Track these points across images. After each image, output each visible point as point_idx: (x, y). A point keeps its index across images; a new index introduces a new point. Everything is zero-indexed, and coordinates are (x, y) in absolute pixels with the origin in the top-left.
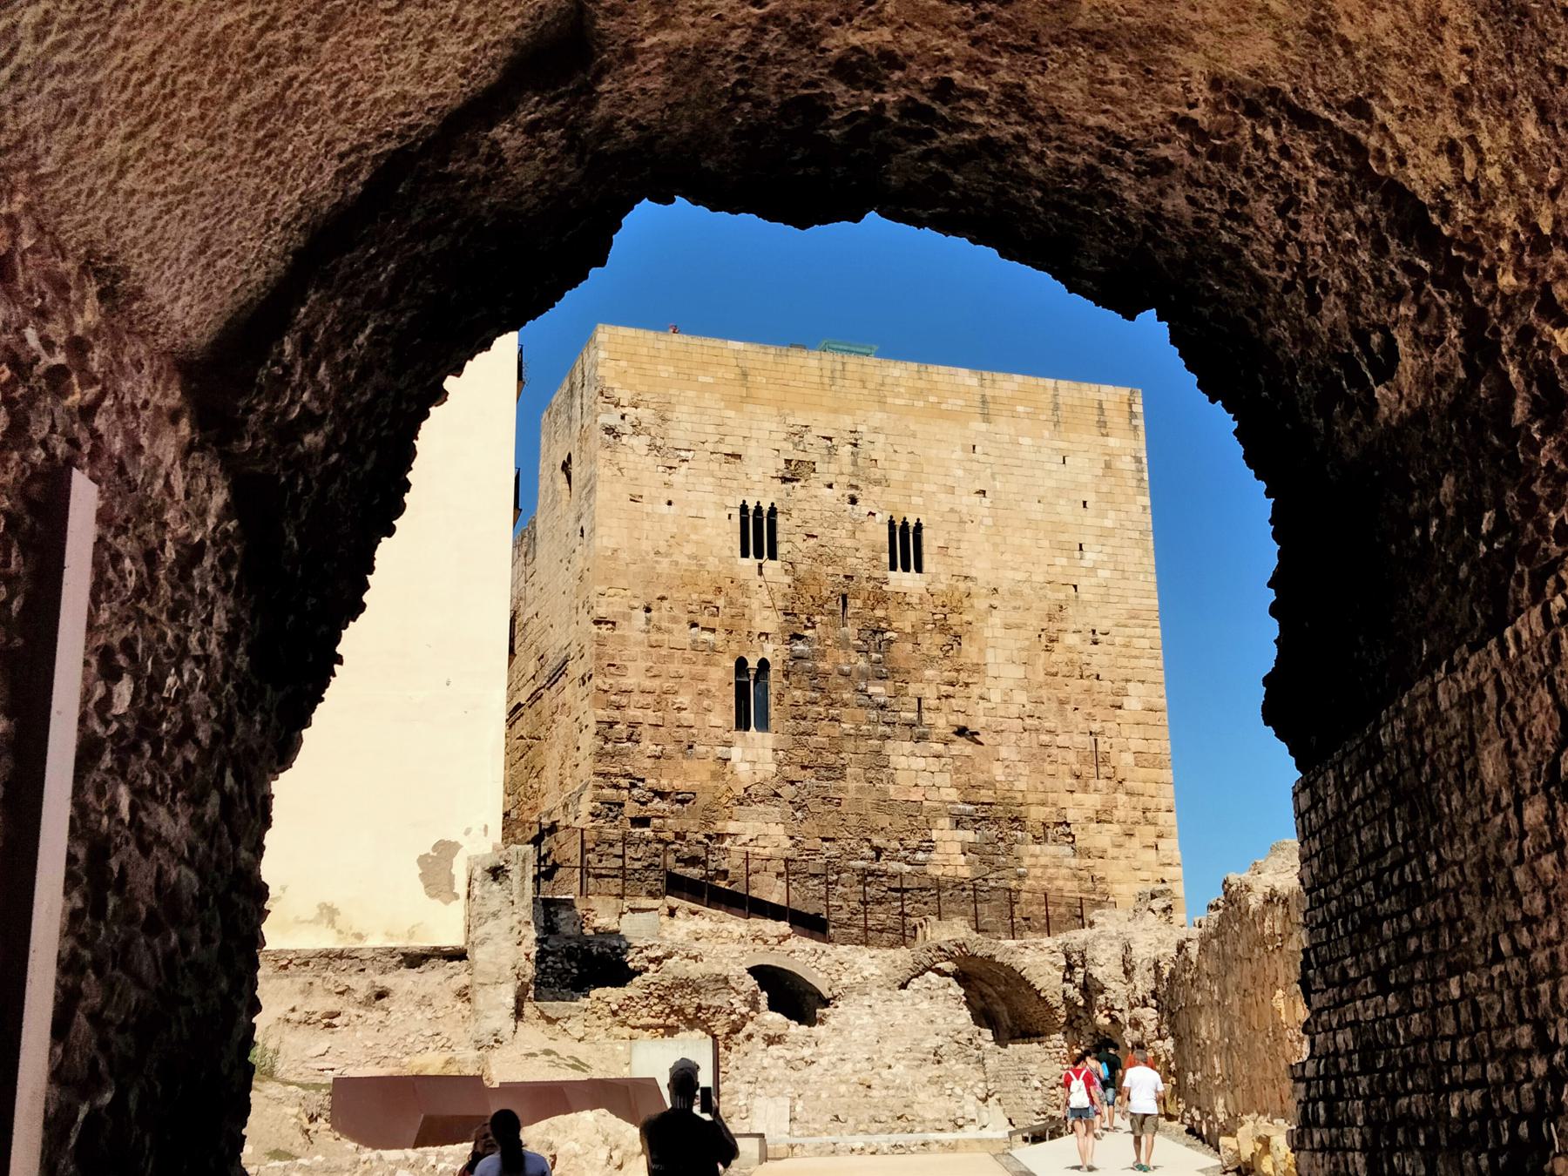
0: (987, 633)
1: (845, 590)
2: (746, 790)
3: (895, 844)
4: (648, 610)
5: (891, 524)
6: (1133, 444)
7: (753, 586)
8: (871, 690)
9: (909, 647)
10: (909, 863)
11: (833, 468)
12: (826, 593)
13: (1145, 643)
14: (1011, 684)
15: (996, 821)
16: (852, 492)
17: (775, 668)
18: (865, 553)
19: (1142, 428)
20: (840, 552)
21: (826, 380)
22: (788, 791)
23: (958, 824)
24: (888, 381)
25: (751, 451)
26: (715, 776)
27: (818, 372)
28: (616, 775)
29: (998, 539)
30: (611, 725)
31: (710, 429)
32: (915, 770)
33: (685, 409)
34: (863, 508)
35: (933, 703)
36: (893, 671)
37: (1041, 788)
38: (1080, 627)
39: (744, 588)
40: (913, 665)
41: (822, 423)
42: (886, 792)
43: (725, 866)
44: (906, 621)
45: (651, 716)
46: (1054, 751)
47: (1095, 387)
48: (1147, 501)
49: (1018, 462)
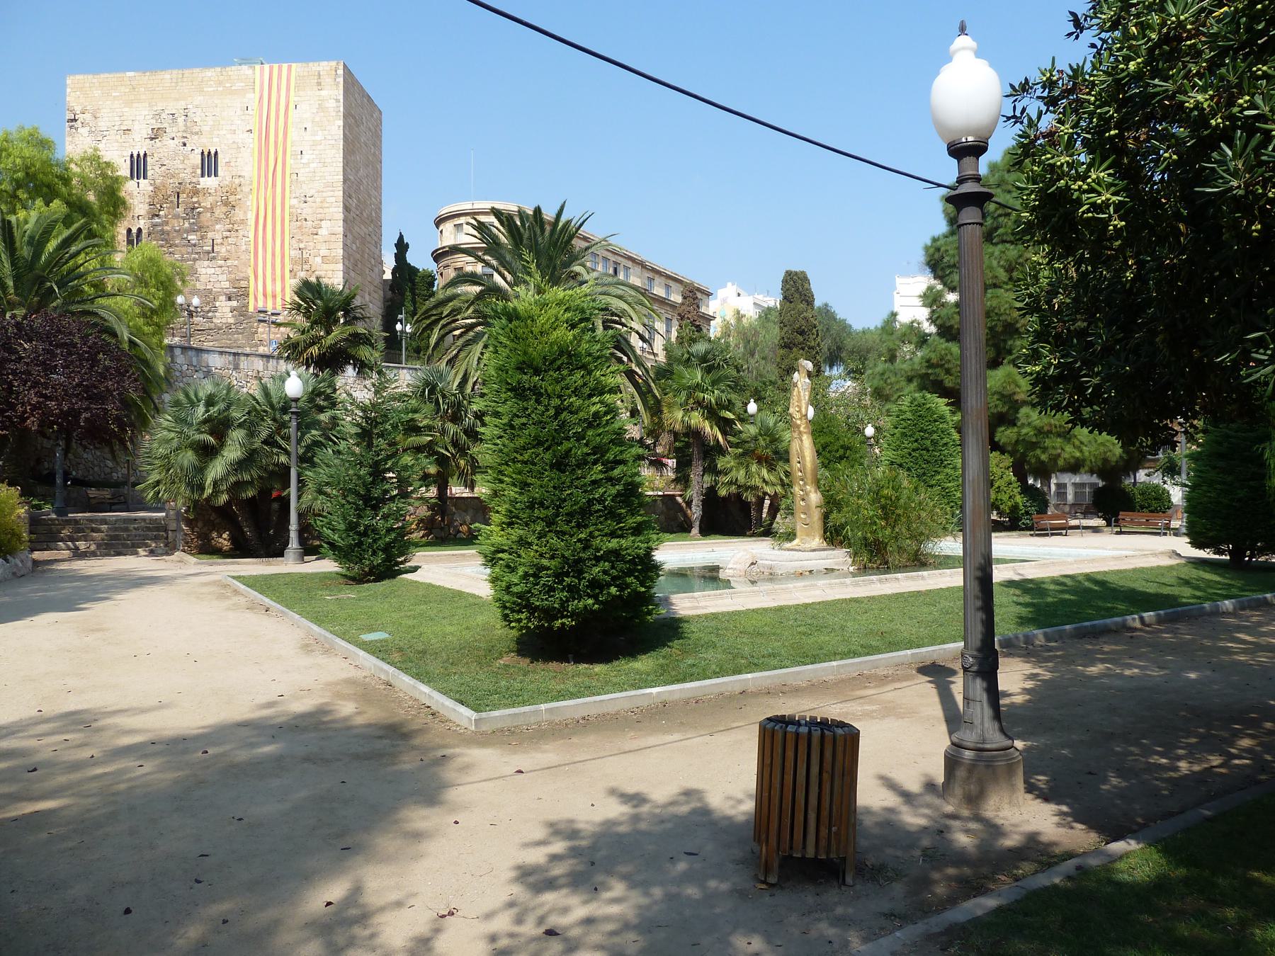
13: (333, 200)
18: (189, 170)
23: (230, 299)
25: (136, 127)
34: (189, 148)
35: (219, 241)
36: (200, 228)
48: (341, 123)
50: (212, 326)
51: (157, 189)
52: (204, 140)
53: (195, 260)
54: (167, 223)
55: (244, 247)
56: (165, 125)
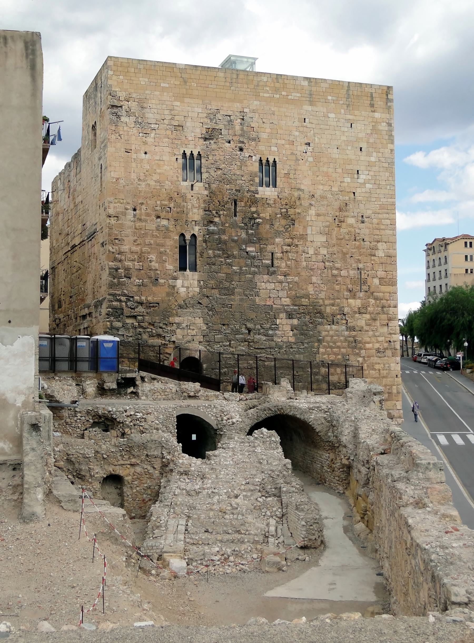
0: (308, 218)
1: (236, 198)
2: (184, 301)
3: (258, 327)
4: (135, 210)
5: (261, 160)
7: (189, 196)
8: (249, 249)
9: (268, 226)
10: (265, 336)
11: (231, 132)
12: (226, 199)
14: (319, 244)
15: (309, 313)
16: (240, 145)
17: (199, 239)
20: (234, 177)
21: (228, 84)
22: (205, 301)
23: (290, 316)
24: (261, 84)
25: (189, 124)
26: (168, 294)
27: (224, 80)
28: (119, 295)
29: (316, 169)
30: (117, 269)
31: (167, 112)
32: (270, 290)
33: (153, 101)
36: (259, 240)
37: (331, 296)
38: (356, 214)
39: (184, 198)
40: (269, 236)
42: (254, 301)
43: (173, 339)
44: (266, 215)
45: (137, 265)
46: (339, 279)
49: (328, 127)
50: (273, 344)
52: (262, 147)
53: (254, 273)
54: (224, 232)
55: (304, 264)
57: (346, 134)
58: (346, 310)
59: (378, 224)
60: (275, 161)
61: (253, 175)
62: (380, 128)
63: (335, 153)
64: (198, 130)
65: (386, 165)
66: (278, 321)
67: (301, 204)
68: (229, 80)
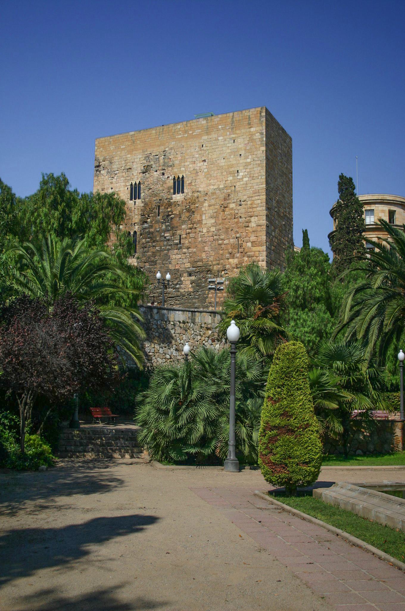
0: (203, 209)
5: (174, 179)
6: (260, 128)
7: (133, 209)
8: (166, 235)
9: (178, 219)
12: (153, 206)
13: (259, 201)
14: (210, 225)
17: (138, 233)
19: (264, 121)
20: (158, 192)
23: (190, 275)
31: (123, 162)
33: (117, 158)
35: (184, 236)
36: (172, 228)
37: (217, 259)
38: (235, 201)
41: (156, 150)
42: (168, 267)
44: (176, 212)
47: (247, 111)
48: (264, 148)
51: (146, 204)
52: (175, 170)
53: (169, 250)
54: (151, 227)
55: (200, 239)
56: (152, 163)
57: (230, 148)
58: (227, 266)
59: (251, 204)
60: (183, 177)
61: (169, 188)
62: (255, 137)
63: (222, 163)
64: (139, 169)
65: (259, 162)
66: (182, 279)
67: (199, 201)
68: (158, 134)
